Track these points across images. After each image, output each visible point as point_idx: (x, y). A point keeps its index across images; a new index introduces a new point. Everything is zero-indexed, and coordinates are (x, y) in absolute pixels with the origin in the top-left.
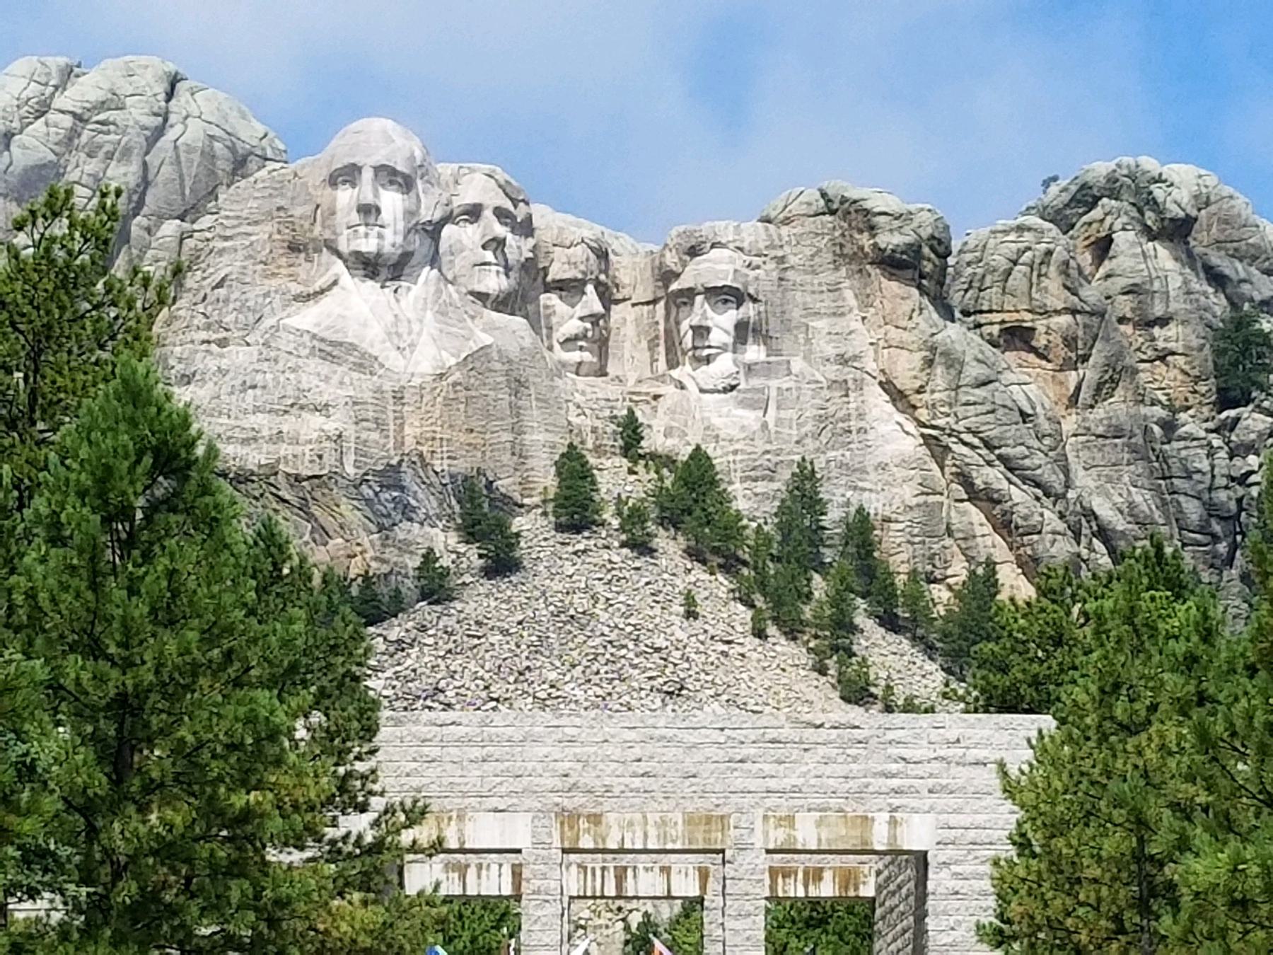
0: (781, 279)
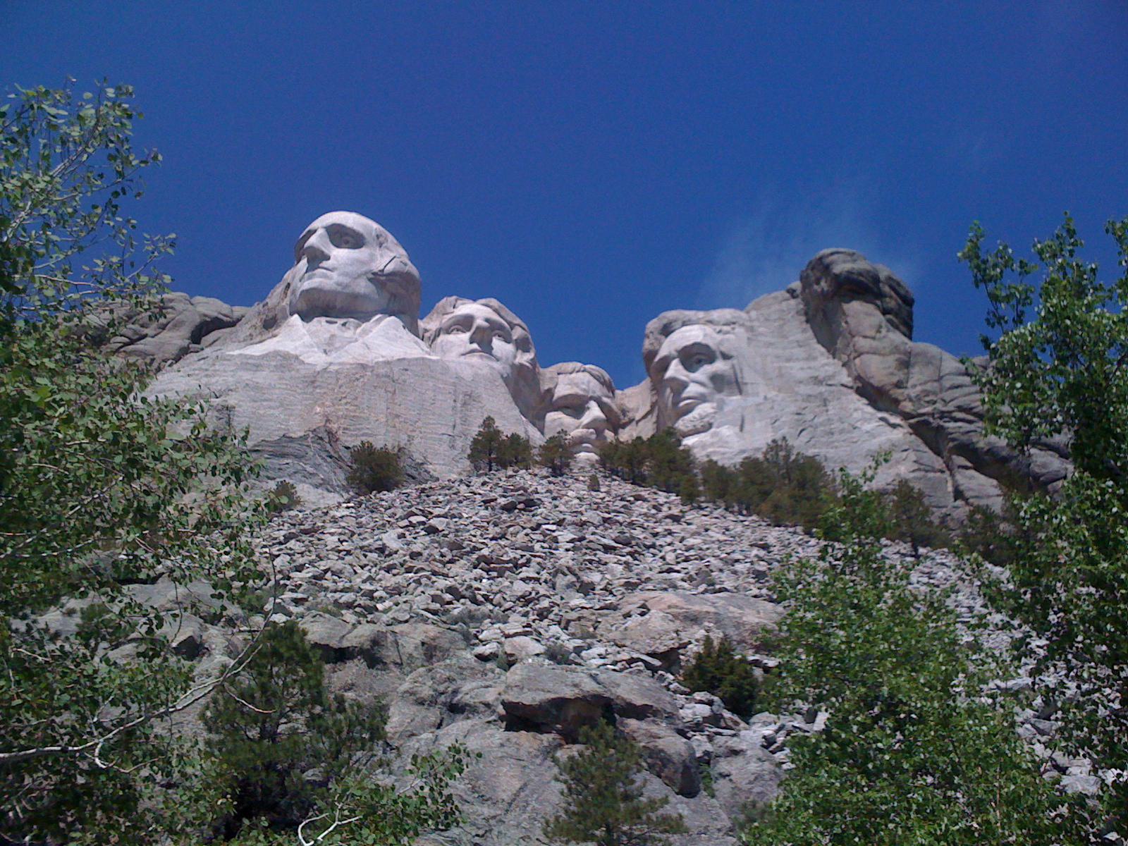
0: (749, 339)
